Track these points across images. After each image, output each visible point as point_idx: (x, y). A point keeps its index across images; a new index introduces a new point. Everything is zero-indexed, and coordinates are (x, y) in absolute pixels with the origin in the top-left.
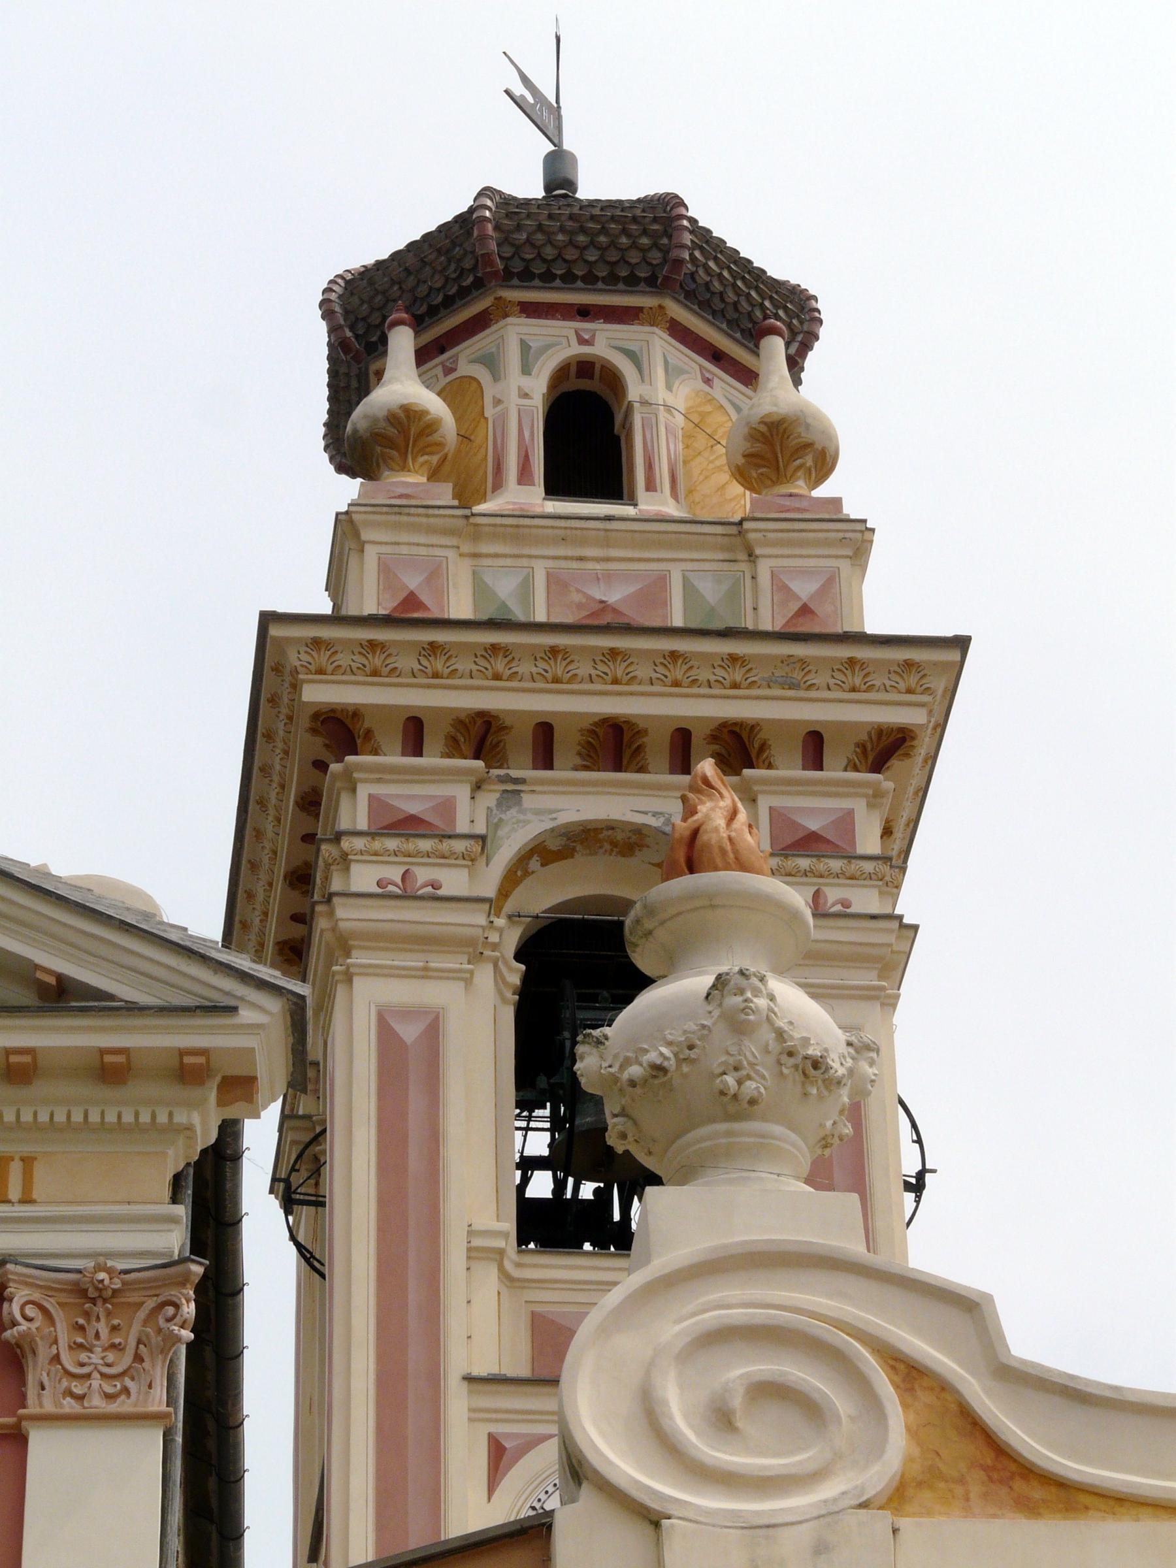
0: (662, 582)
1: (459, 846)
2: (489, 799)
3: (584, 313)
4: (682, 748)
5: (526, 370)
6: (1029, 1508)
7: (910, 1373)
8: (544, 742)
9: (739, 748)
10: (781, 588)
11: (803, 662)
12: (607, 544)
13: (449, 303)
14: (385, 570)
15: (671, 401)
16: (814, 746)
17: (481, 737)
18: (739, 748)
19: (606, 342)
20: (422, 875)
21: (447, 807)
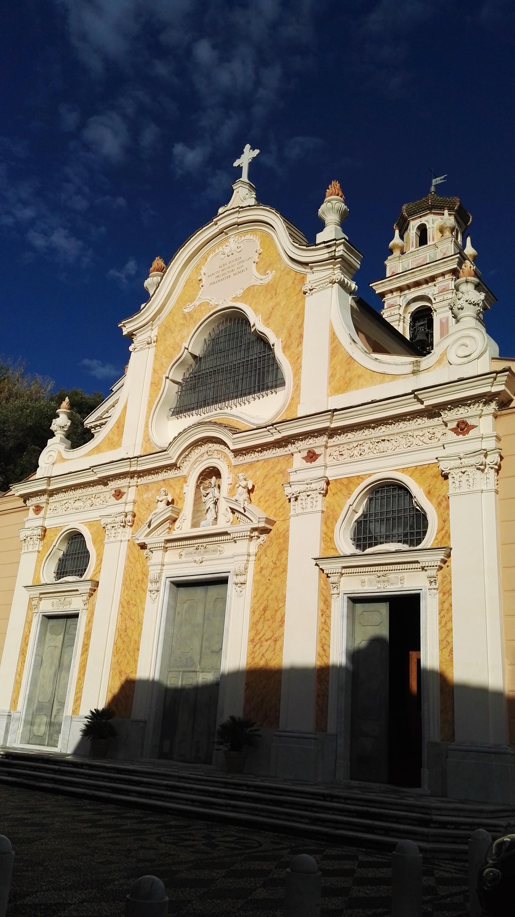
0: (426, 256)
1: (449, 291)
2: (402, 298)
3: (420, 217)
4: (427, 281)
5: (413, 230)
6: (63, 462)
7: (59, 452)
8: (408, 287)
9: (433, 279)
10: (441, 251)
11: (438, 264)
12: (418, 254)
13: (404, 222)
14: (390, 269)
15: (433, 226)
16: (443, 274)
17: (401, 289)
18: (433, 279)
19: (423, 220)
20: (393, 312)
21: (396, 302)
